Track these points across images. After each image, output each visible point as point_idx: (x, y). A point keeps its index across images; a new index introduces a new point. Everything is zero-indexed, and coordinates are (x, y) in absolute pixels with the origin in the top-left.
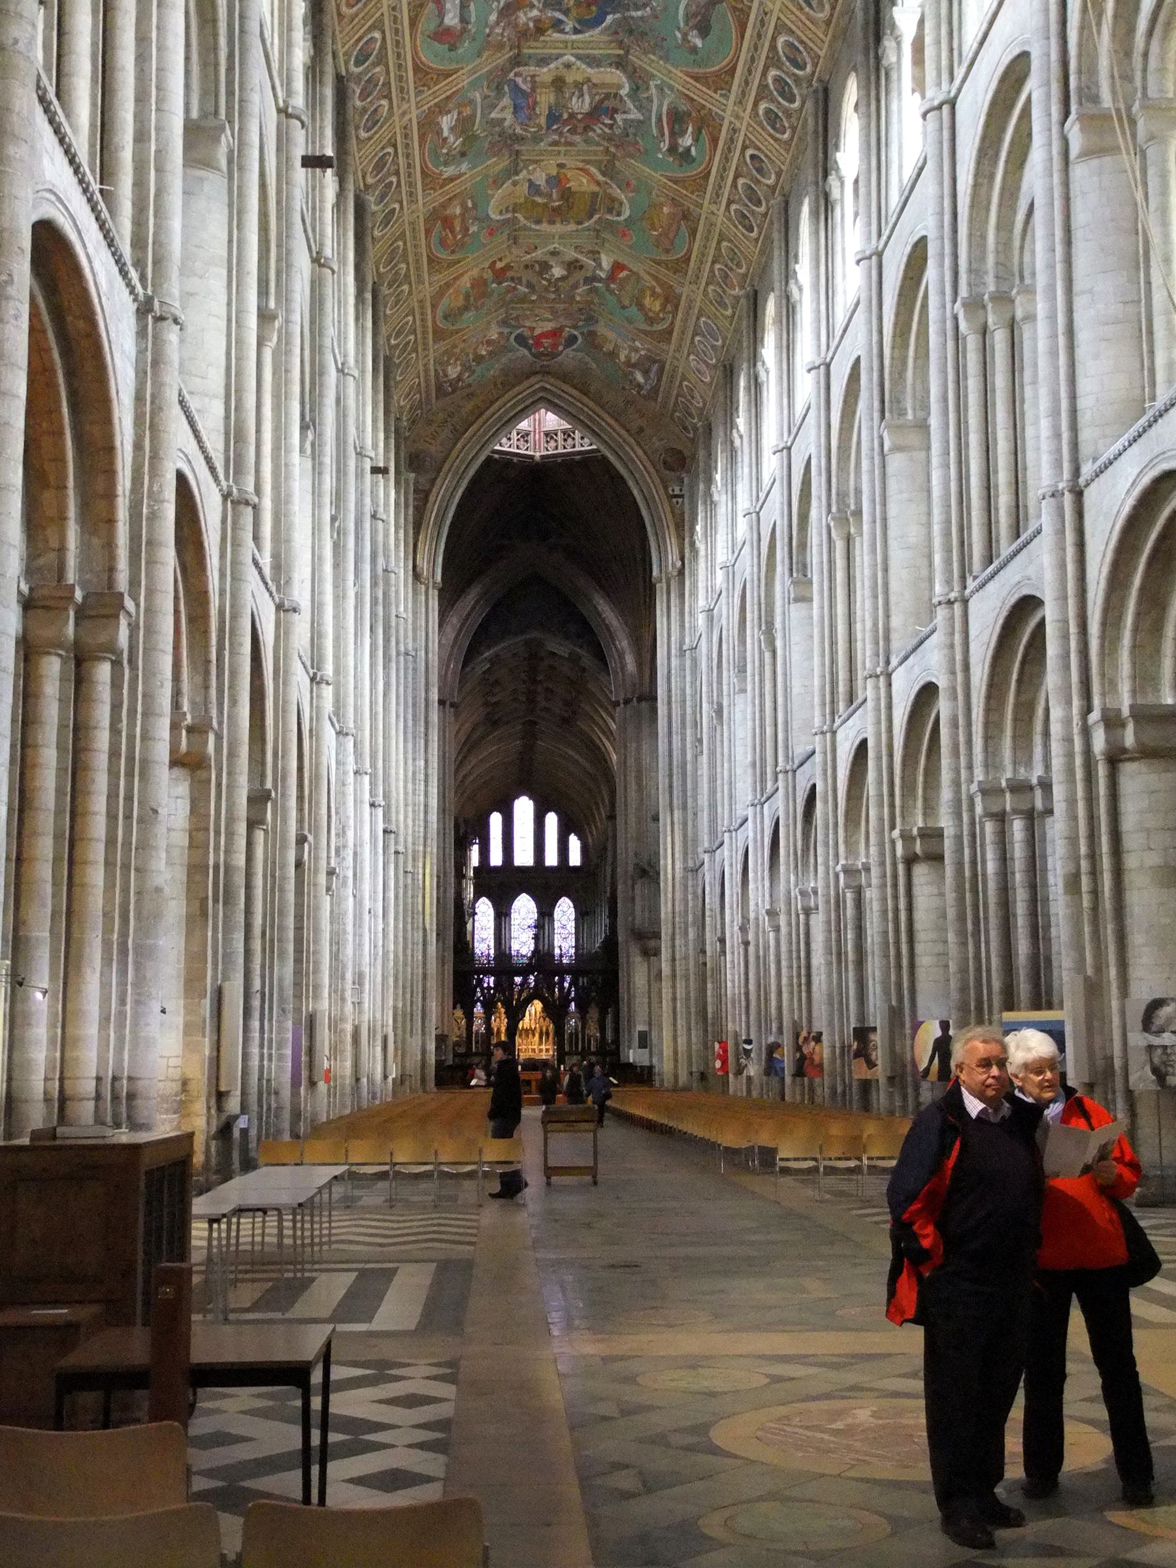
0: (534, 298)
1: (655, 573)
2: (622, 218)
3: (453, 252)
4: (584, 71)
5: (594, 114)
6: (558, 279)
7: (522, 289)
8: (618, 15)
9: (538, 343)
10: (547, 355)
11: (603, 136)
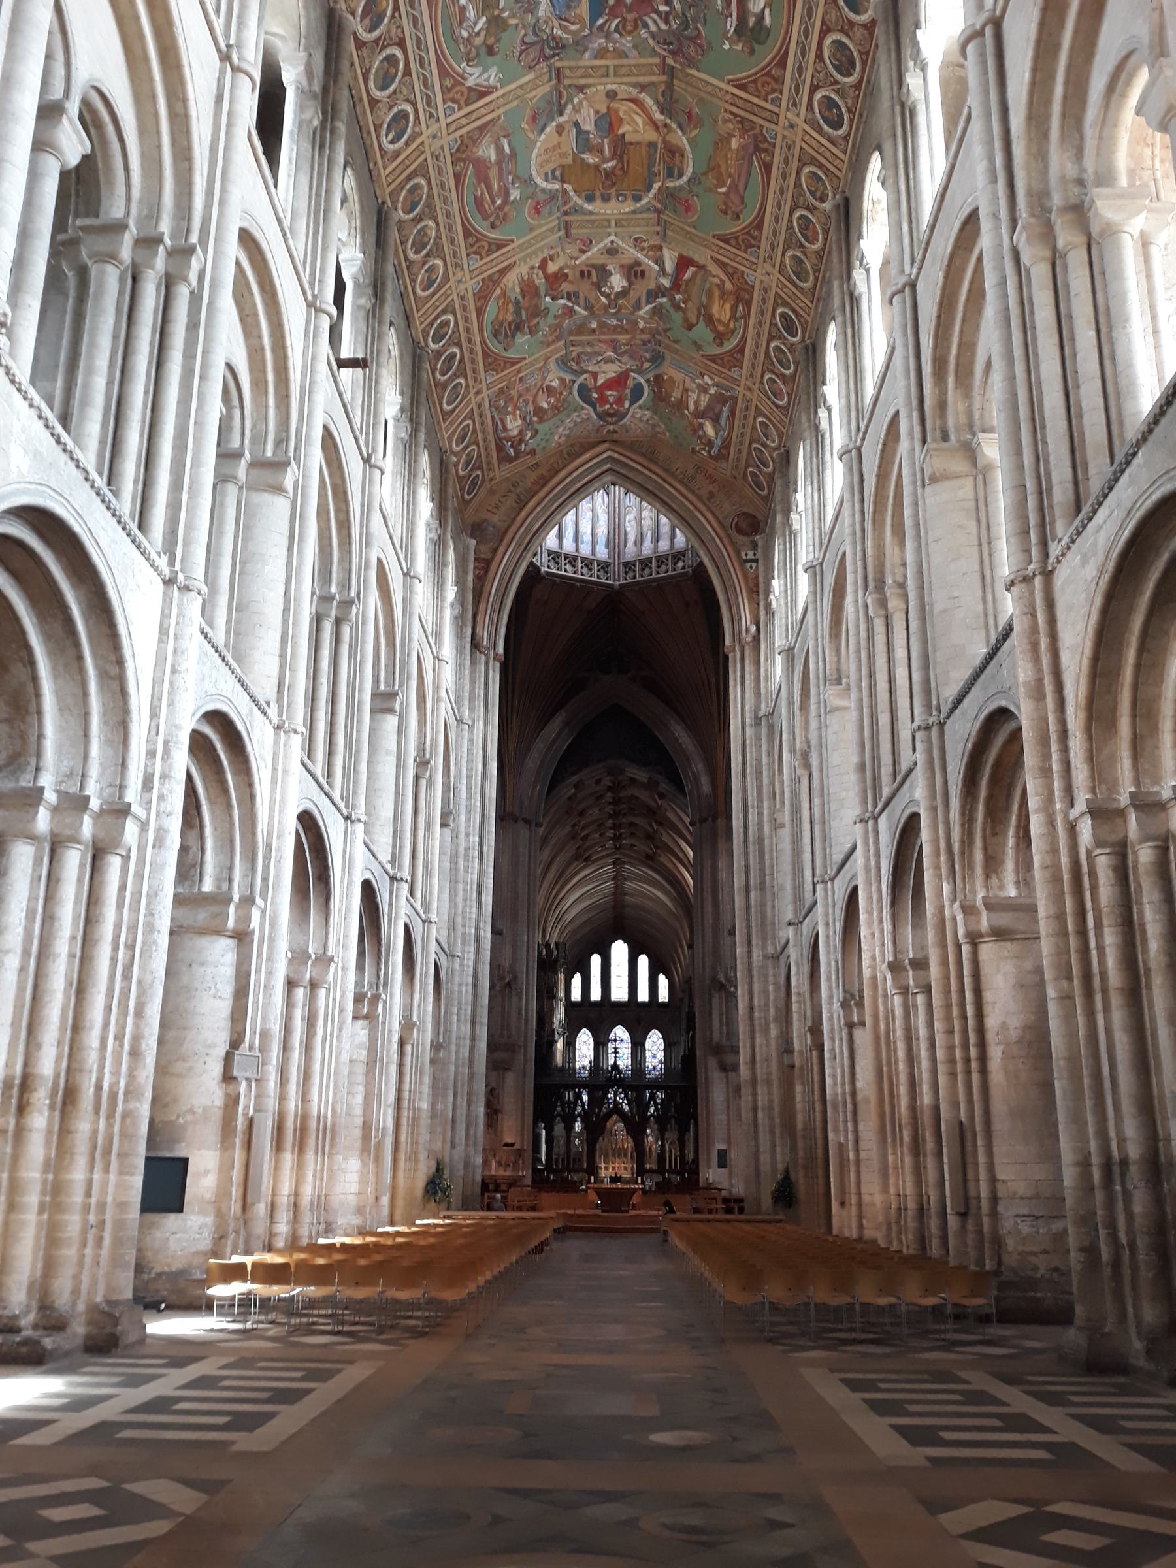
0: (594, 325)
2: (685, 179)
3: (493, 226)
6: (618, 294)
9: (603, 399)
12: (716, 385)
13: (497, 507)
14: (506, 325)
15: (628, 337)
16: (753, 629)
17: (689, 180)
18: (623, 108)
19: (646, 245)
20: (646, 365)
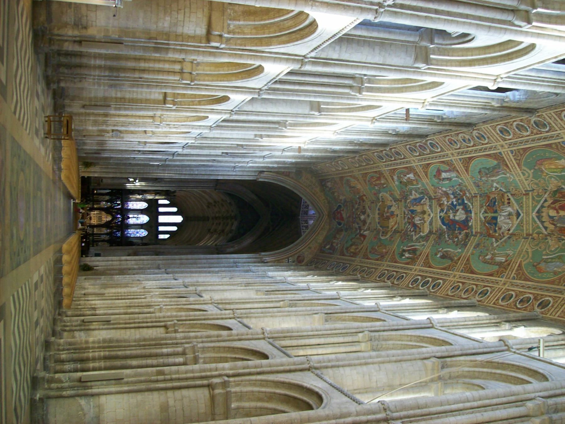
1: (263, 253)
3: (369, 181)
5: (415, 225)
7: (356, 206)
11: (407, 228)
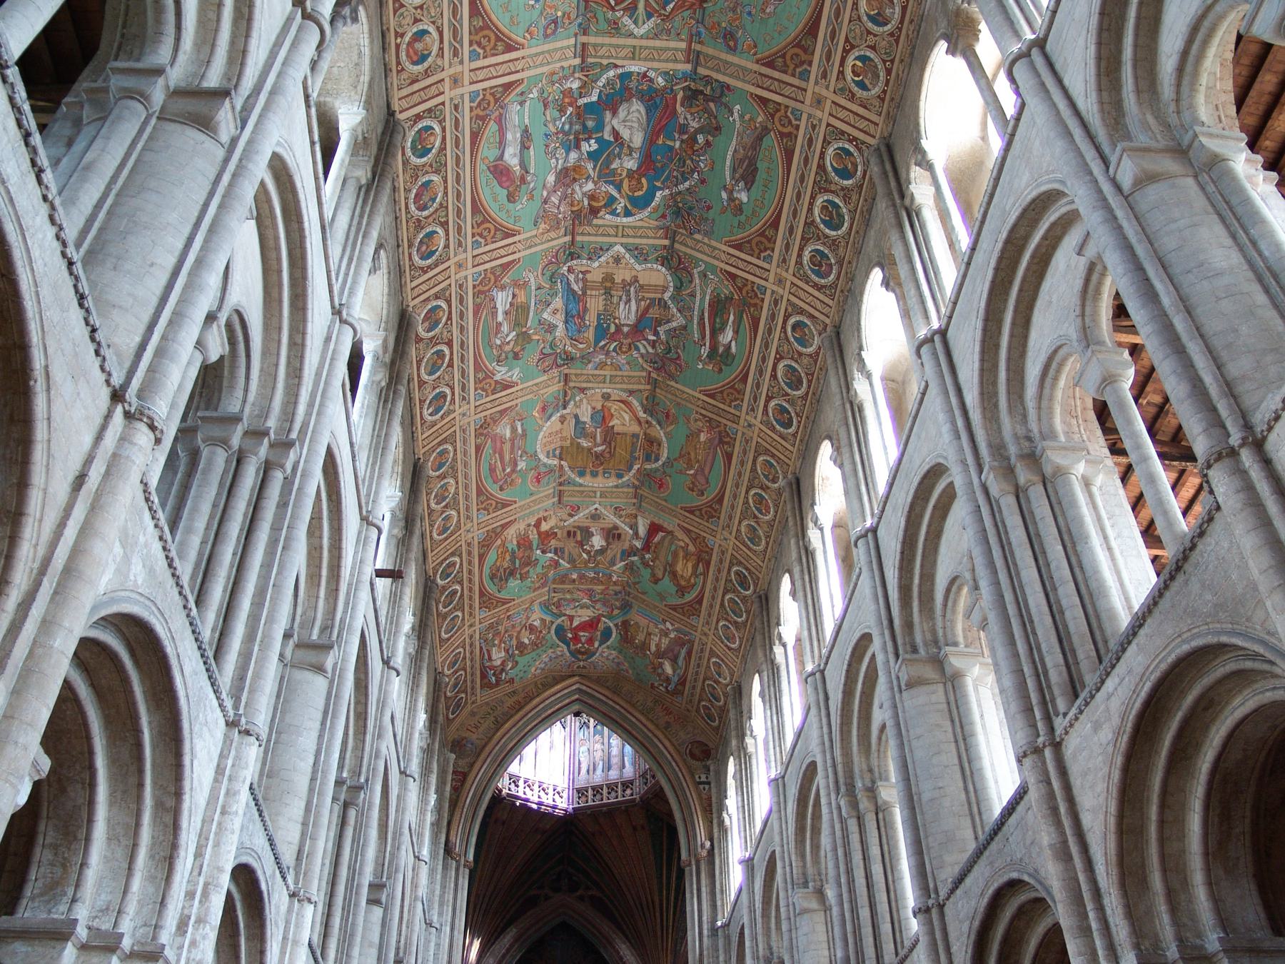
0: (575, 576)
2: (660, 462)
3: (501, 489)
4: (633, 268)
5: (637, 329)
8: (667, 192)
9: (576, 639)
10: (583, 654)
12: (677, 630)
13: (477, 727)
14: (502, 570)
15: (603, 587)
16: (708, 844)
17: (663, 464)
18: (614, 407)
19: (624, 513)
20: (616, 612)
